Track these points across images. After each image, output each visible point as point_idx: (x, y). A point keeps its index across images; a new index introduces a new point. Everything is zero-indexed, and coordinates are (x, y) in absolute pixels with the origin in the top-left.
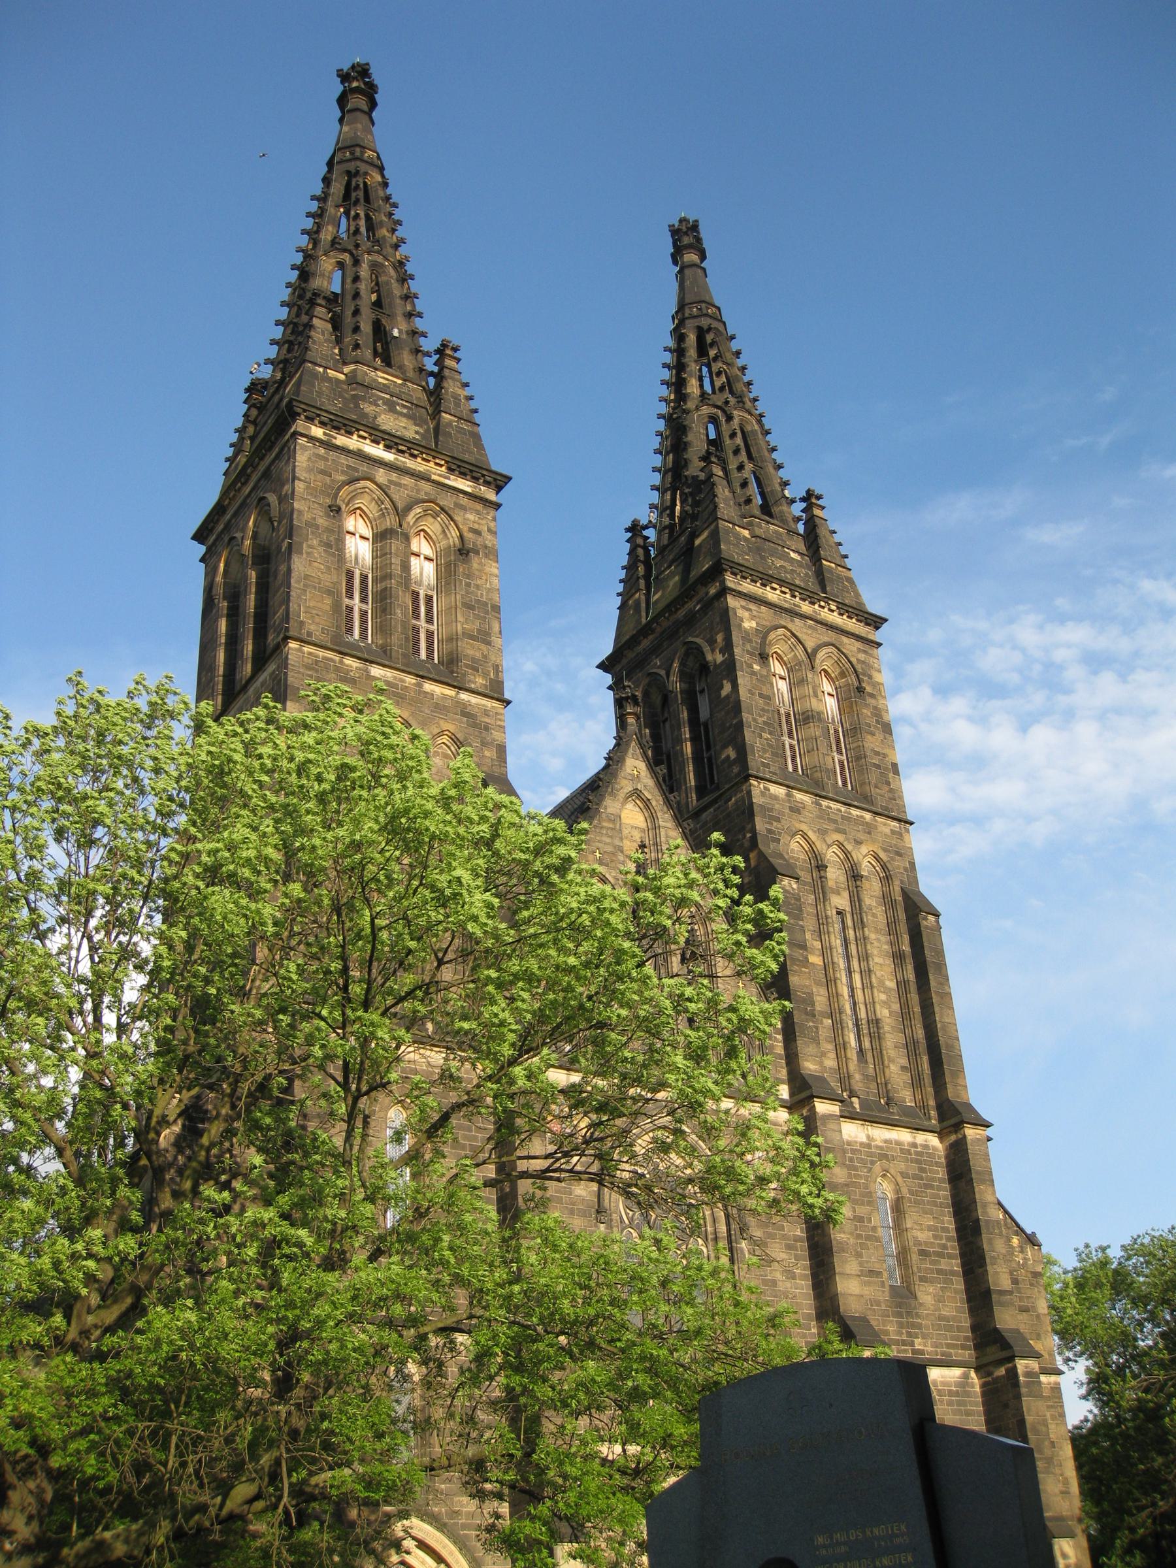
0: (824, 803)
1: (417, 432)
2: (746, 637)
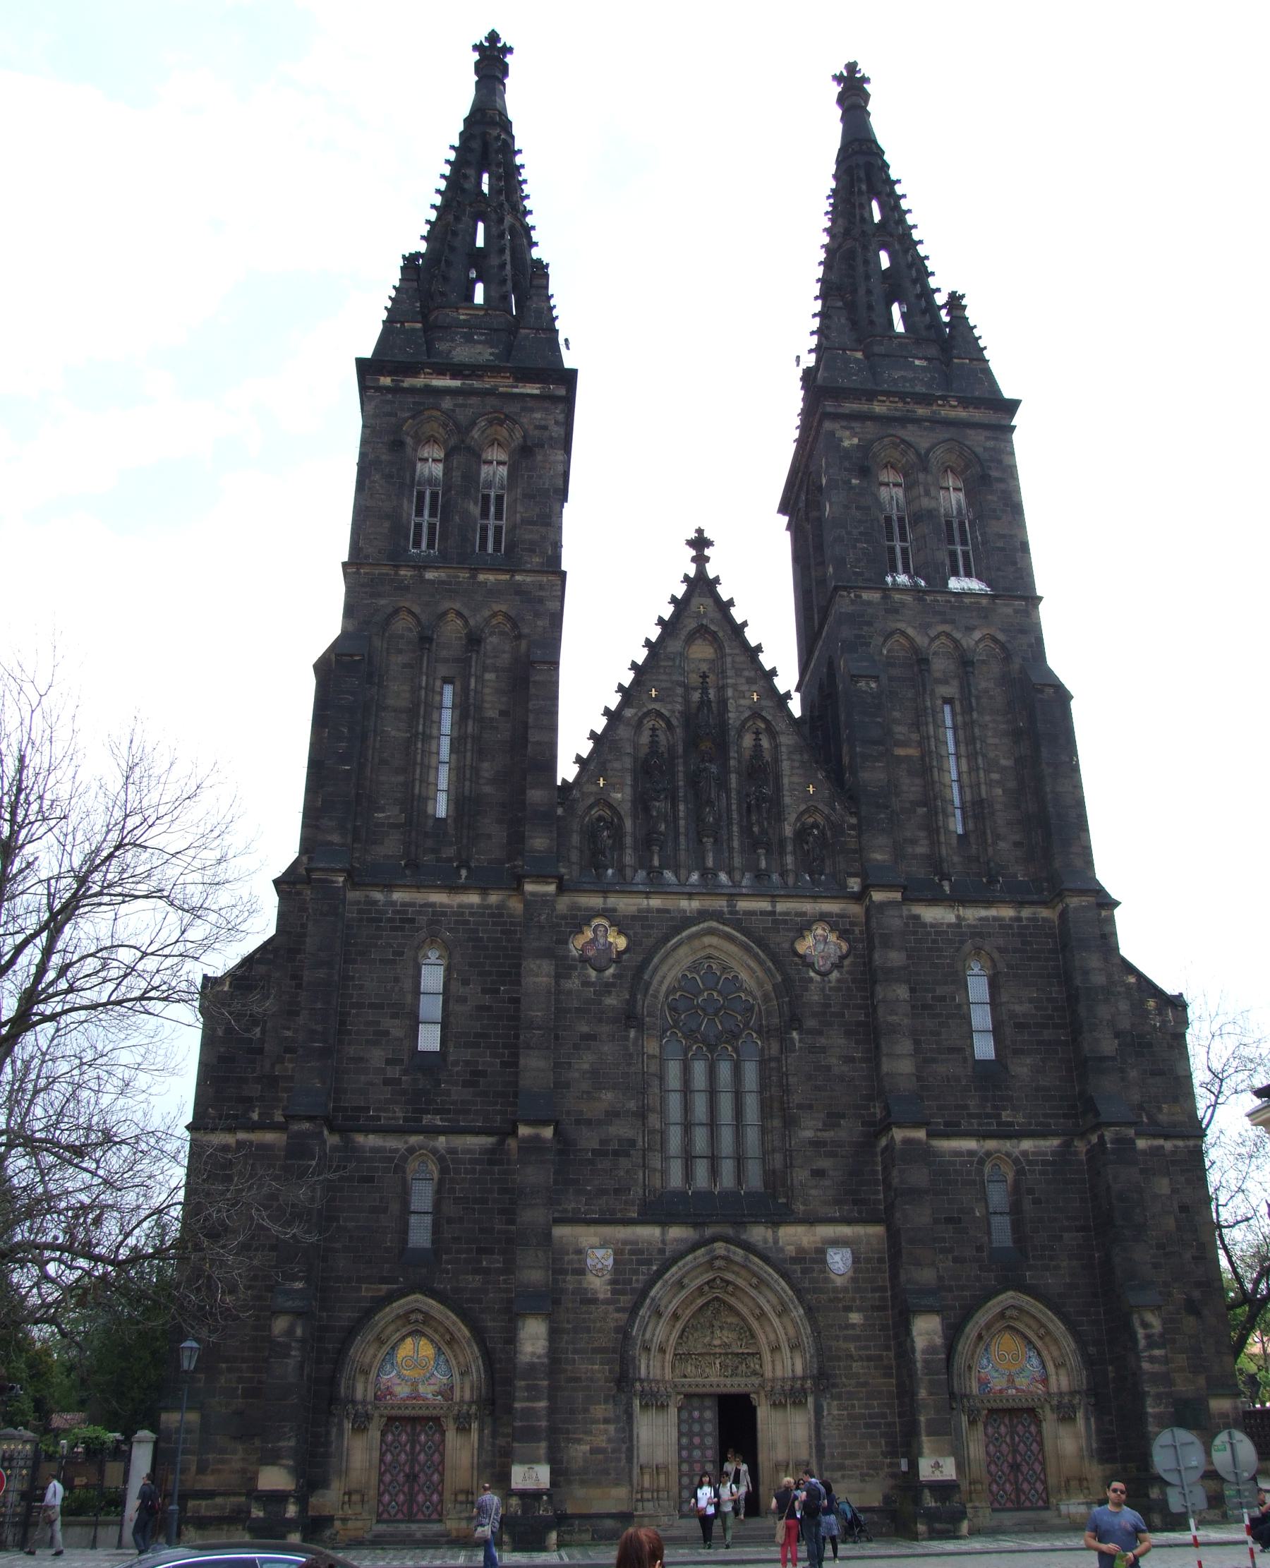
1: (491, 354)
2: (846, 454)
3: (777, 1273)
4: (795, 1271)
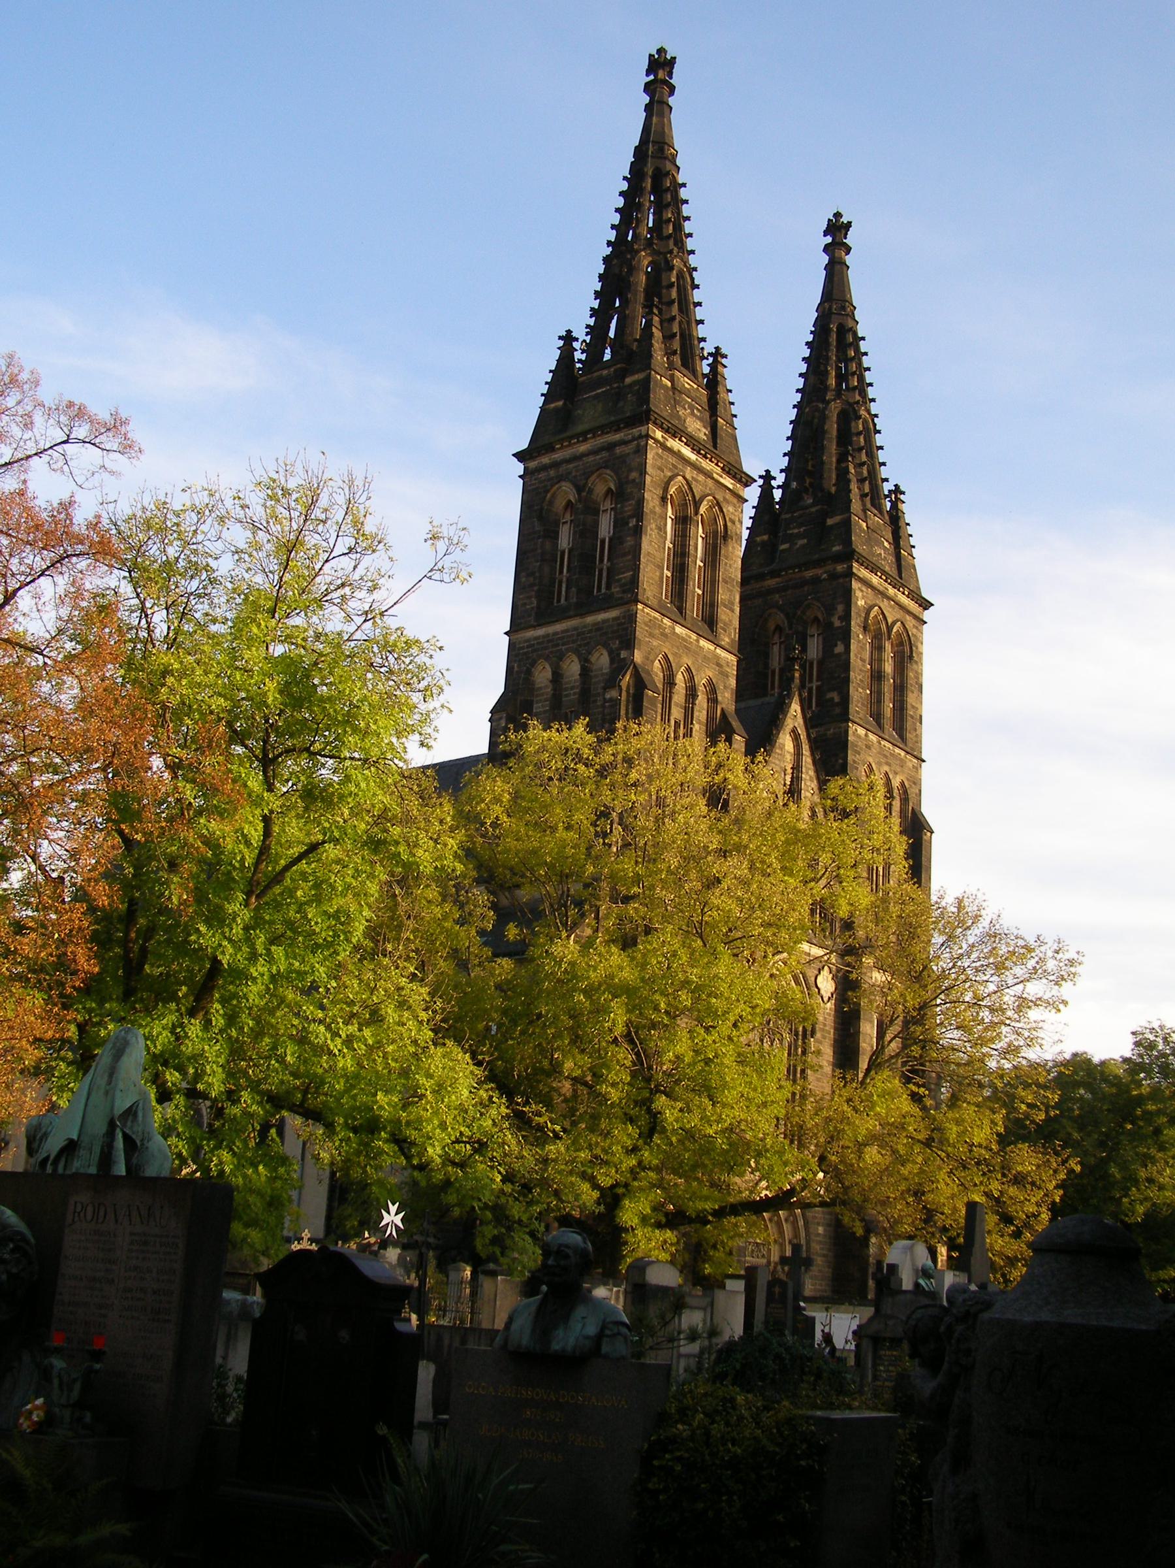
0: (883, 742)
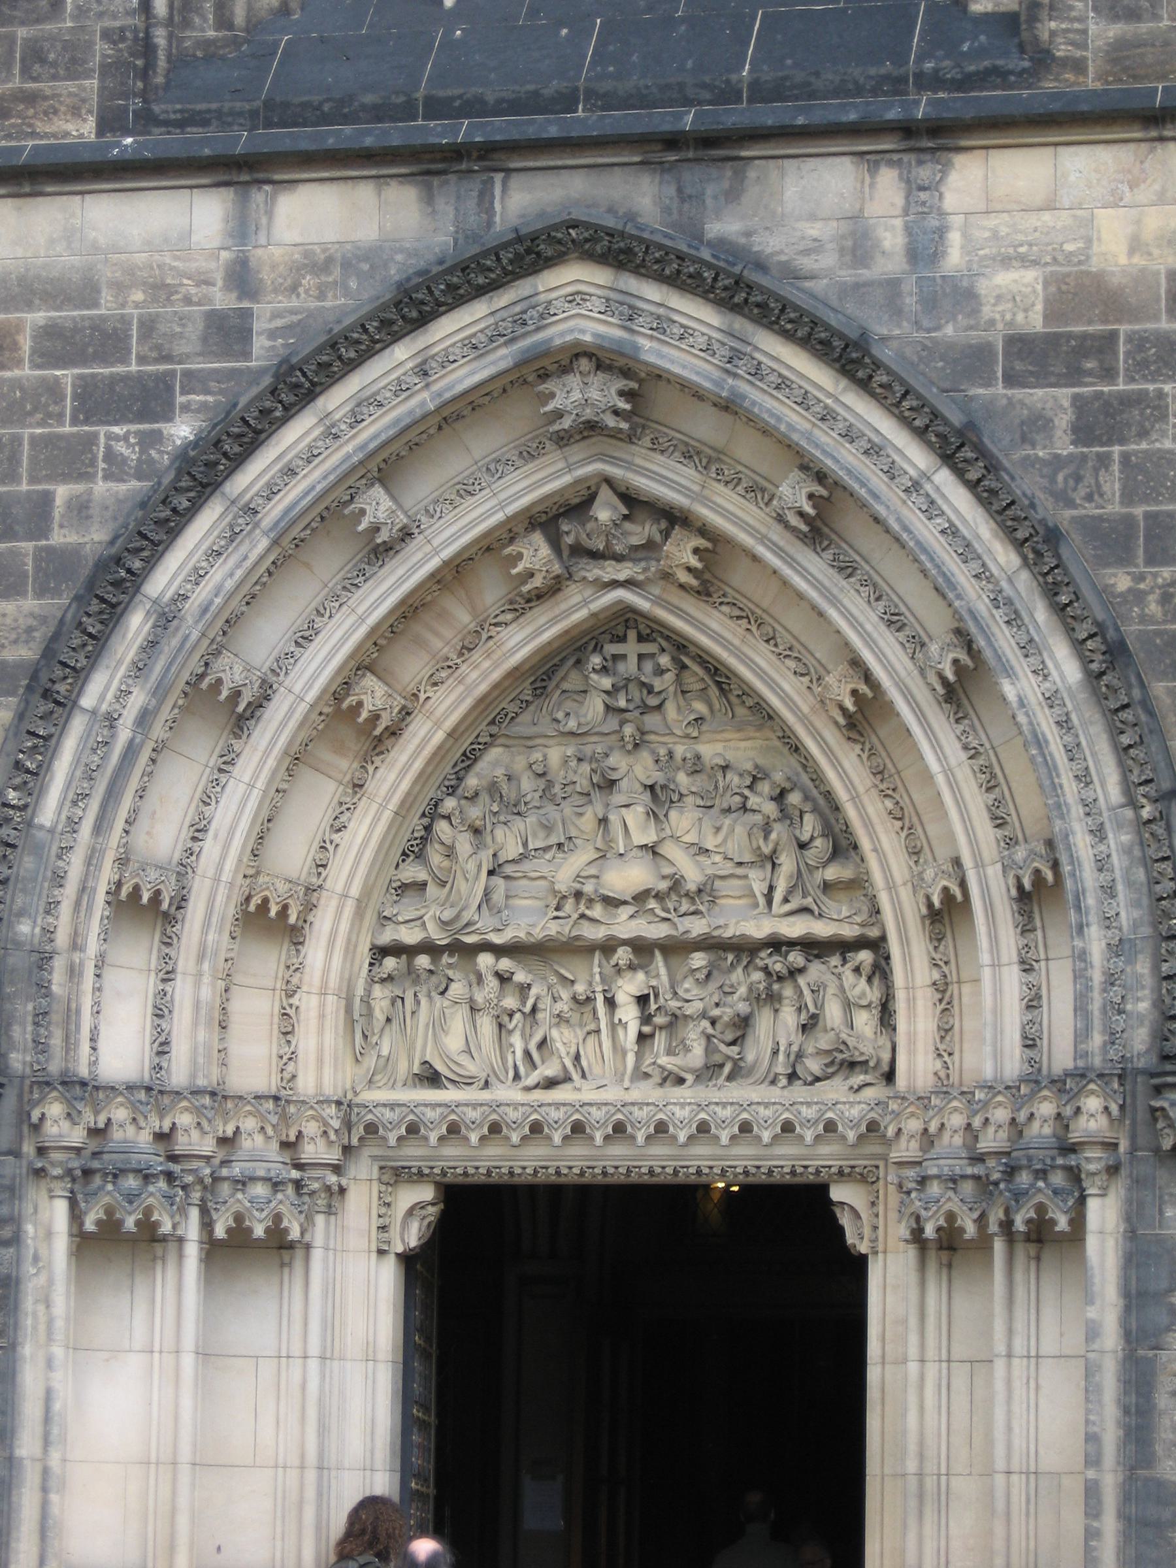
3: (920, 433)
4: (1037, 425)
